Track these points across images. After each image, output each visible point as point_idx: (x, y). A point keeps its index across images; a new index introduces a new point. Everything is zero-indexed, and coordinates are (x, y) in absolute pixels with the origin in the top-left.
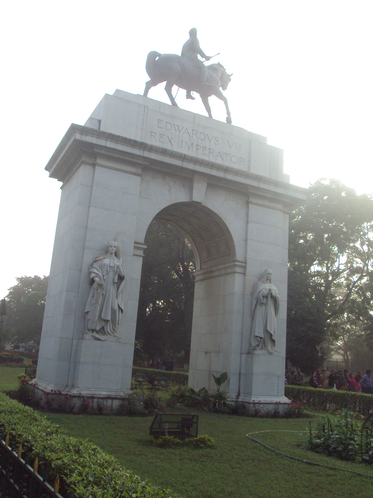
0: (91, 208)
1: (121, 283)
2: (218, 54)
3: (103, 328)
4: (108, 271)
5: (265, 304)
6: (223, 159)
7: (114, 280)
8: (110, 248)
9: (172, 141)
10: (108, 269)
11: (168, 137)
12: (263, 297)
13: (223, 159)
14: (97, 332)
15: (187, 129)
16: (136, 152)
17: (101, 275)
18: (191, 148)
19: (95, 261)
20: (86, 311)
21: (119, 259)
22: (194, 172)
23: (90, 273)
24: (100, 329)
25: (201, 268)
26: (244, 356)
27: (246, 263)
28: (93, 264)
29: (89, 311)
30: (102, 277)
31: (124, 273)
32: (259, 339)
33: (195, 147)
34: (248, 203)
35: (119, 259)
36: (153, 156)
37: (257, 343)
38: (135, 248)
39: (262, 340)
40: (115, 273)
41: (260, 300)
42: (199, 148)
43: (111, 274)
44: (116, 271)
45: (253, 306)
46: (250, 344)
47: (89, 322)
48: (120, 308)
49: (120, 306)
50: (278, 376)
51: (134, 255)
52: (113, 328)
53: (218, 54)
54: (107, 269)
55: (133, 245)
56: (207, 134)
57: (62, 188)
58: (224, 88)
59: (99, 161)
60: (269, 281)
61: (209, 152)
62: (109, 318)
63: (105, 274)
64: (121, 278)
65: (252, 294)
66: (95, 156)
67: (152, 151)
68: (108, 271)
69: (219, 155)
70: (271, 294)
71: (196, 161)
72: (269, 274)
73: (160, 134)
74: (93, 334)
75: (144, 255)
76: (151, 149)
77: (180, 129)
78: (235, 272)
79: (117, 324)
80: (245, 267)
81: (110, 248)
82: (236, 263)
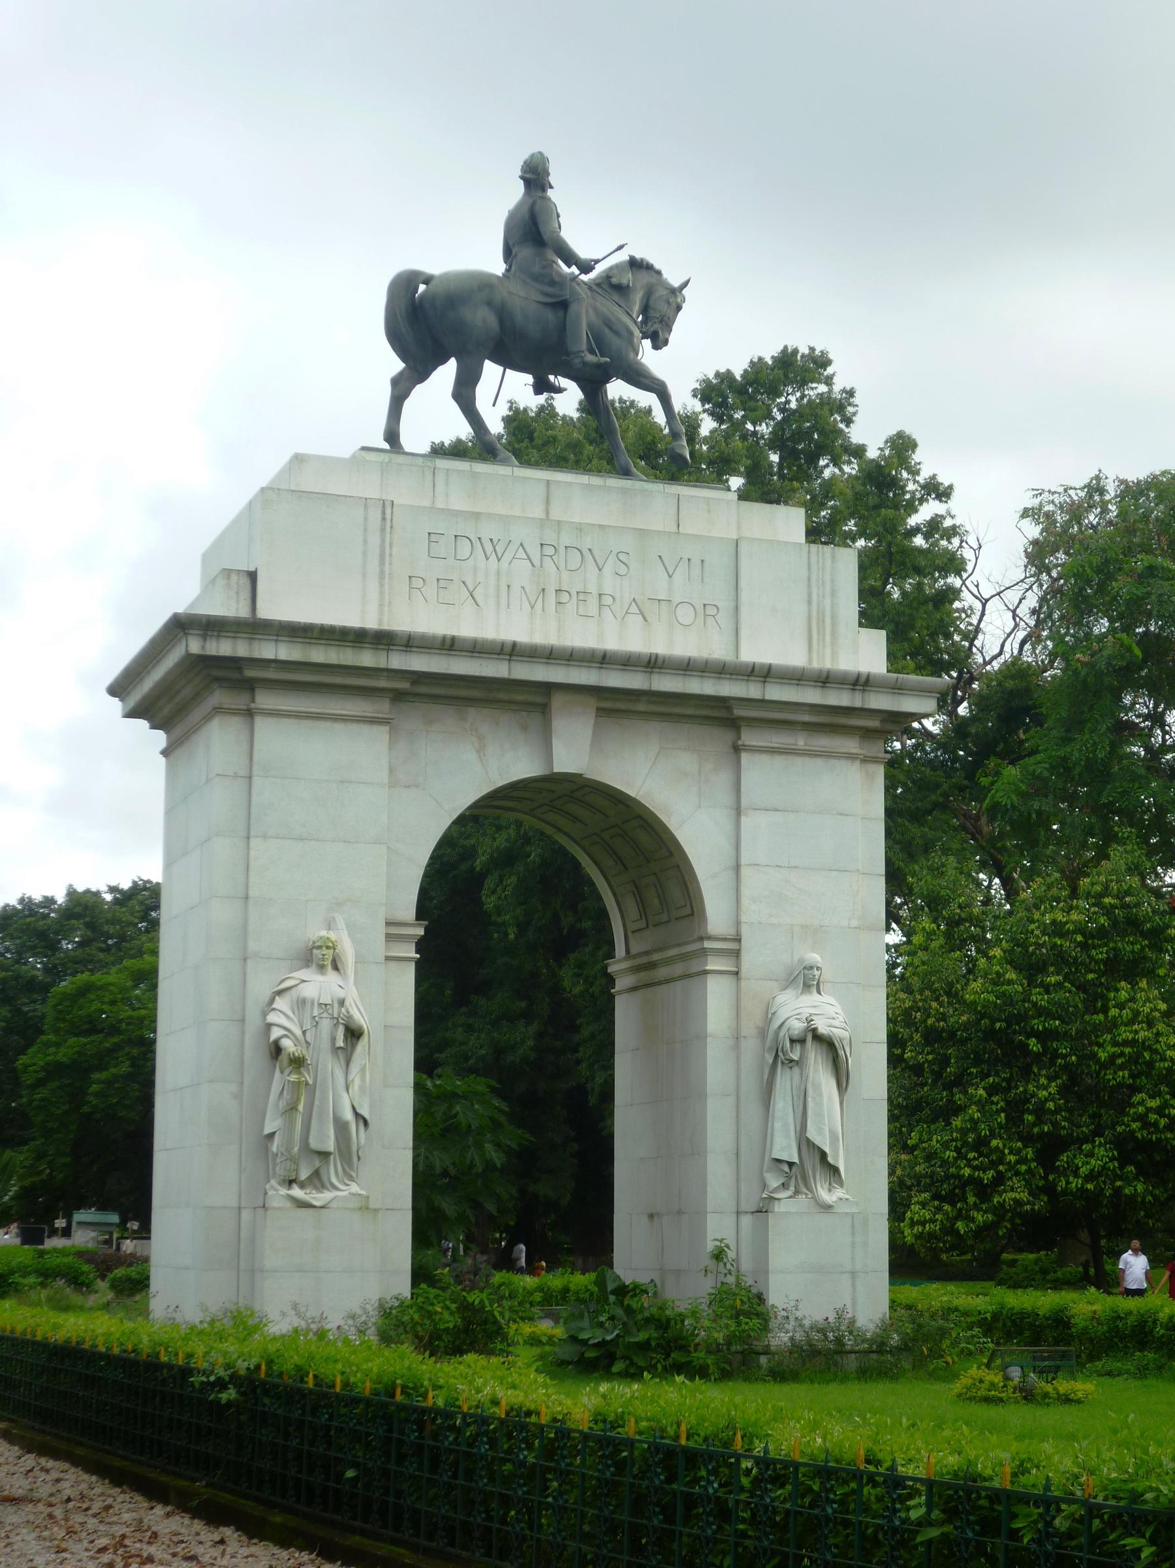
0: (253, 842)
1: (354, 1047)
3: (316, 1174)
4: (317, 1019)
5: (799, 1063)
6: (645, 620)
7: (333, 1040)
8: (315, 951)
9: (475, 594)
10: (316, 1013)
11: (464, 582)
12: (792, 1041)
13: (645, 620)
14: (302, 1186)
15: (521, 544)
16: (367, 658)
17: (298, 1032)
18: (539, 604)
19: (280, 993)
20: (267, 1131)
21: (344, 976)
22: (549, 688)
23: (269, 1026)
24: (309, 1178)
25: (628, 951)
26: (746, 1220)
27: (739, 941)
28: (272, 1001)
29: (274, 1133)
30: (301, 1037)
31: (360, 1018)
32: (786, 1168)
33: (551, 598)
34: (737, 749)
35: (344, 976)
36: (419, 663)
37: (782, 1180)
38: (389, 937)
39: (794, 1169)
40: (335, 1021)
41: (783, 1048)
42: (565, 597)
43: (326, 1024)
44: (339, 1016)
45: (767, 1071)
46: (764, 1186)
47: (278, 1160)
48: (357, 1115)
49: (358, 1111)
51: (388, 958)
52: (344, 1169)
54: (312, 1013)
55: (381, 930)
56: (590, 550)
57: (165, 753)
58: (659, 342)
59: (265, 700)
60: (814, 990)
61: (601, 606)
62: (331, 1146)
63: (307, 1026)
64: (354, 1034)
65: (763, 1032)
66: (250, 686)
67: (413, 649)
68: (317, 1019)
69: (634, 609)
70: (814, 1030)
71: (551, 655)
72: (811, 968)
73: (438, 580)
74: (290, 1192)
75: (418, 956)
76: (410, 643)
77: (499, 549)
78: (706, 972)
79: (355, 1159)
80: (736, 954)
81: (315, 951)
82: (707, 944)
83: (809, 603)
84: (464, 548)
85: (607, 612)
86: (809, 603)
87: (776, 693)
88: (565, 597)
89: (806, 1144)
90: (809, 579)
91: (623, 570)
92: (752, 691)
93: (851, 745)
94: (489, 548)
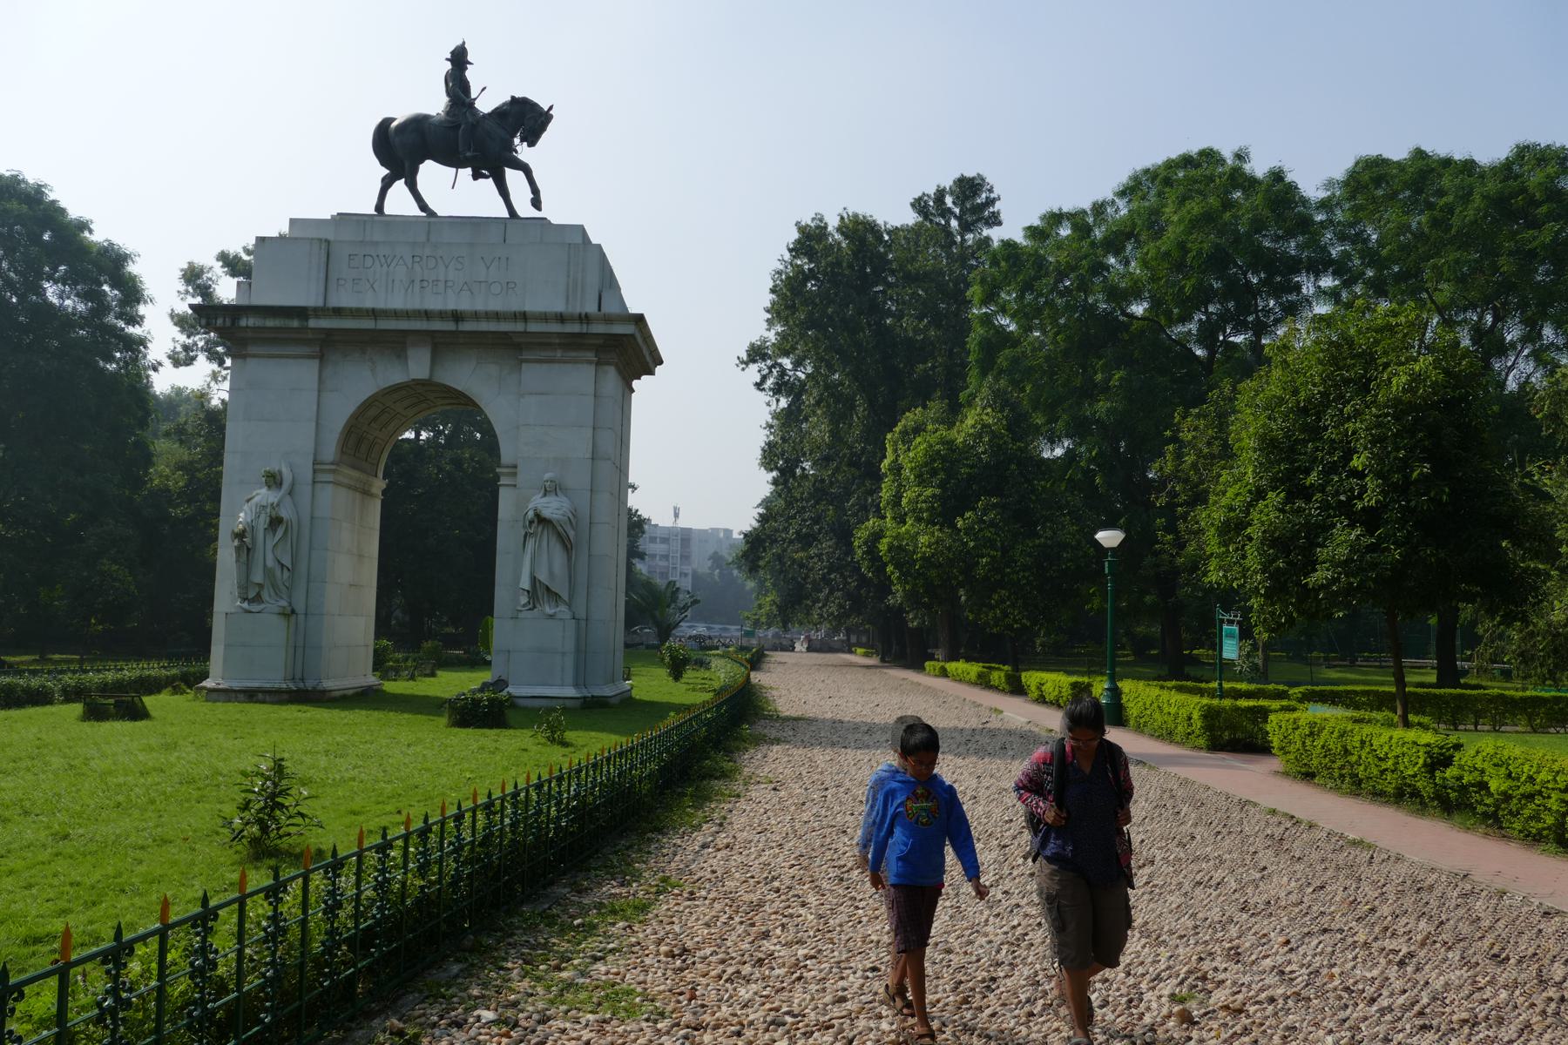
2: (484, 89)
18: (410, 290)
27: (515, 467)
33: (417, 285)
38: (315, 471)
50: (563, 654)
53: (484, 89)
59: (252, 349)
61: (446, 287)
77: (389, 261)
83: (568, 276)
84: (369, 261)
85: (449, 290)
86: (568, 276)
87: (533, 327)
88: (425, 284)
89: (534, 580)
90: (569, 263)
91: (460, 267)
92: (519, 327)
93: (591, 355)
94: (383, 260)
